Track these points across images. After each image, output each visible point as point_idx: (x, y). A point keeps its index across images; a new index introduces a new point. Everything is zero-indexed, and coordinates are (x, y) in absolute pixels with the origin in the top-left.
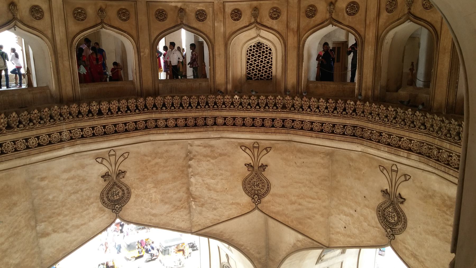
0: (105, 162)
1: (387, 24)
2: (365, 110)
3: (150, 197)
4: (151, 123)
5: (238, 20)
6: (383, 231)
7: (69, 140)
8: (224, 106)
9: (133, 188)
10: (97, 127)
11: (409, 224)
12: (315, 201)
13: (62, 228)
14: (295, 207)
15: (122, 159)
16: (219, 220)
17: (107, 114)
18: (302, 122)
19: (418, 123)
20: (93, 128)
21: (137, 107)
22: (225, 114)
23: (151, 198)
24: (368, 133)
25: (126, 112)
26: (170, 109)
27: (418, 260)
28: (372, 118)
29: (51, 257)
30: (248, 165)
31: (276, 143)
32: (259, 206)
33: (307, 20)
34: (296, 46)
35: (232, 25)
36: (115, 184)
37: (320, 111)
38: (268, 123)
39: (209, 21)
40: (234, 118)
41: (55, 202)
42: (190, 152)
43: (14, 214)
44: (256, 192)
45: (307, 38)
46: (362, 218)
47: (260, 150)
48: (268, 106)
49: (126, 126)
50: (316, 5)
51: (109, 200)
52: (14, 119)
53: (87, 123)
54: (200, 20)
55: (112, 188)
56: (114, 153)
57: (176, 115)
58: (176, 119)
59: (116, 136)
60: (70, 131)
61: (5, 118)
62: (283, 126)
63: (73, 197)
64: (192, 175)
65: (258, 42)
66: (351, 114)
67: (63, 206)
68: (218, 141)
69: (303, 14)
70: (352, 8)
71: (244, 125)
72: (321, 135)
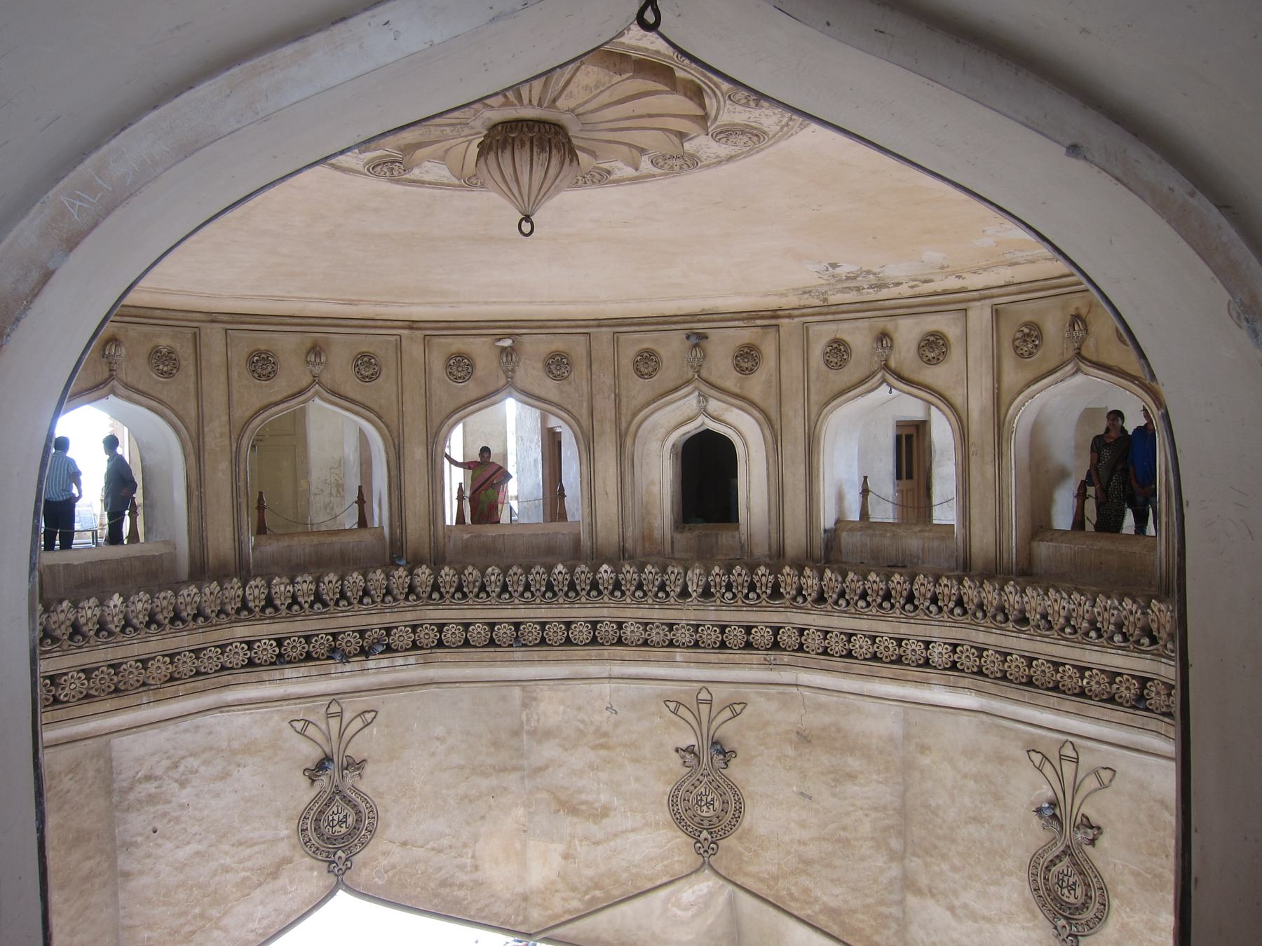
0: (1047, 769)
7: (945, 669)
9: (1116, 896)
41: (939, 821)
43: (845, 798)
63: (972, 828)
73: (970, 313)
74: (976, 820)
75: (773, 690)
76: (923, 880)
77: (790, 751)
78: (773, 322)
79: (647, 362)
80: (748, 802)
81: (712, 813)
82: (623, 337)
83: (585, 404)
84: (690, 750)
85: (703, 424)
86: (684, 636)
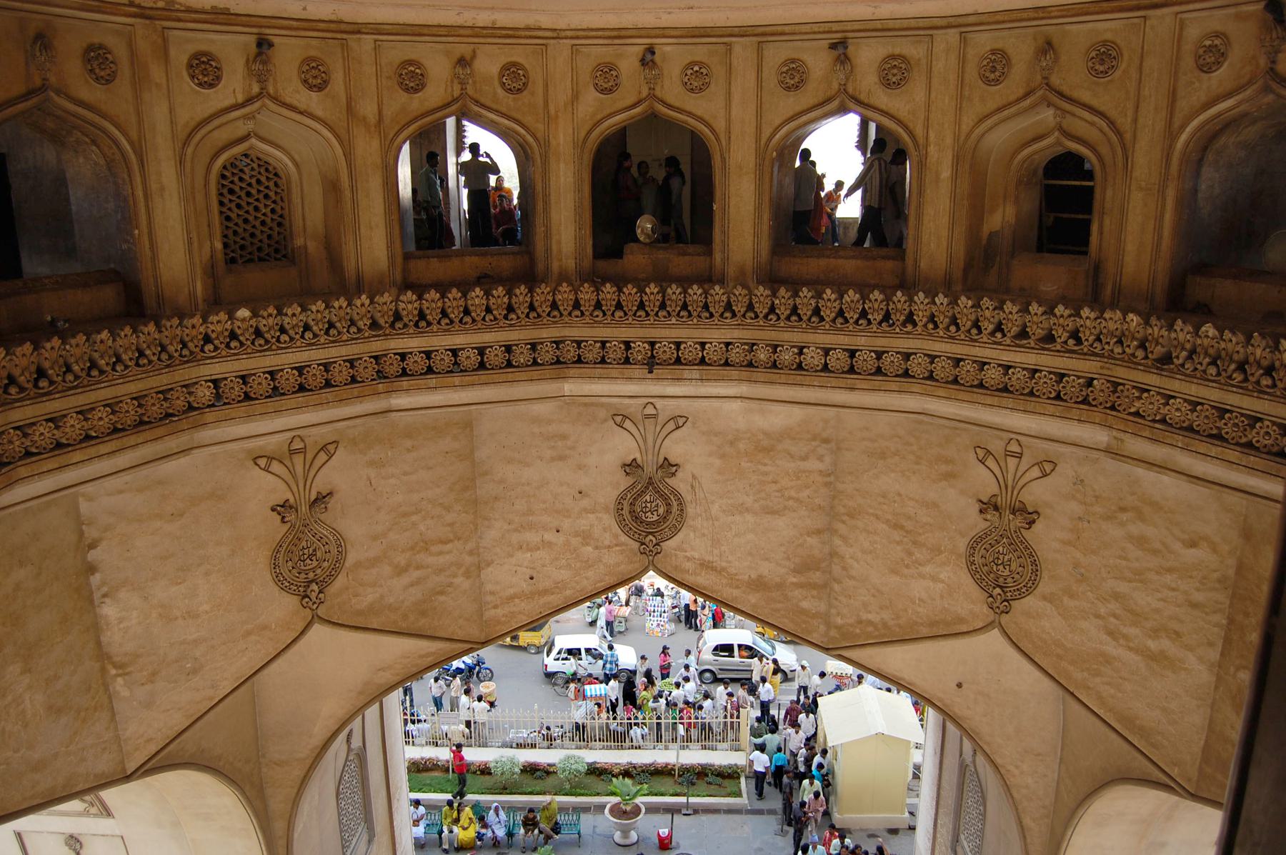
1: (599, 117)
2: (582, 302)
4: (11, 442)
5: (211, 86)
6: (636, 545)
11: (690, 510)
12: (449, 546)
14: (406, 579)
16: (211, 698)
18: (428, 354)
19: (716, 309)
27: (714, 569)
28: (605, 314)
30: (282, 509)
31: (348, 427)
33: (403, 97)
34: (379, 161)
44: (311, 575)
46: (575, 541)
47: (309, 456)
50: (424, 61)
62: (381, 375)
64: (105, 596)
66: (549, 315)
70: (516, 76)
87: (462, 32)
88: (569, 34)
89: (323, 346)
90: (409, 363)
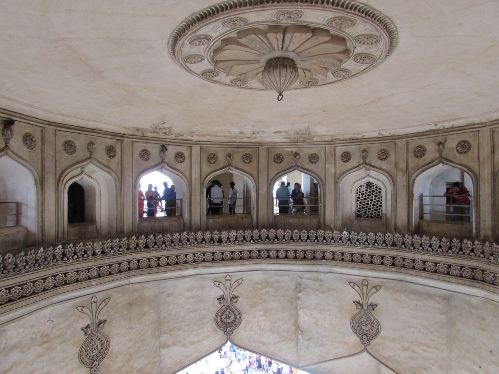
2: (485, 251)
3: (260, 324)
4: (264, 253)
5: (347, 161)
7: (192, 263)
8: (332, 241)
9: (244, 313)
10: (216, 253)
13: (180, 342)
15: (236, 284)
17: (226, 242)
18: (414, 261)
20: (213, 254)
21: (252, 237)
22: (333, 248)
23: (260, 325)
24: (491, 277)
25: (242, 241)
26: (282, 241)
29: (169, 368)
31: (386, 282)
32: (368, 348)
33: (416, 160)
35: (342, 166)
36: (228, 307)
37: (433, 250)
38: (377, 260)
39: (320, 163)
40: (342, 254)
42: (300, 285)
44: (365, 332)
45: (417, 176)
47: (369, 288)
48: (378, 243)
49: (241, 254)
51: (222, 322)
52: (151, 240)
53: (208, 249)
54: (312, 163)
55: (225, 311)
56: (230, 278)
57: (285, 247)
58: (286, 251)
59: (232, 262)
60: (194, 254)
61: (144, 239)
62: (393, 265)
64: (301, 308)
65: (367, 181)
66: (469, 254)
67: (183, 322)
68: (327, 275)
69: (411, 154)
70: (463, 147)
71: (352, 261)
72: (436, 276)
73: (193, 148)
74: (194, 311)
75: (119, 289)
76: (170, 341)
77: (126, 312)
78: (122, 139)
79: (69, 147)
80: (111, 340)
81: (97, 352)
82: (58, 133)
83: (40, 163)
84: (88, 327)
85: (82, 178)
86: (95, 273)
87: (439, 132)
88: (489, 124)
89: (371, 249)
90: (406, 263)
